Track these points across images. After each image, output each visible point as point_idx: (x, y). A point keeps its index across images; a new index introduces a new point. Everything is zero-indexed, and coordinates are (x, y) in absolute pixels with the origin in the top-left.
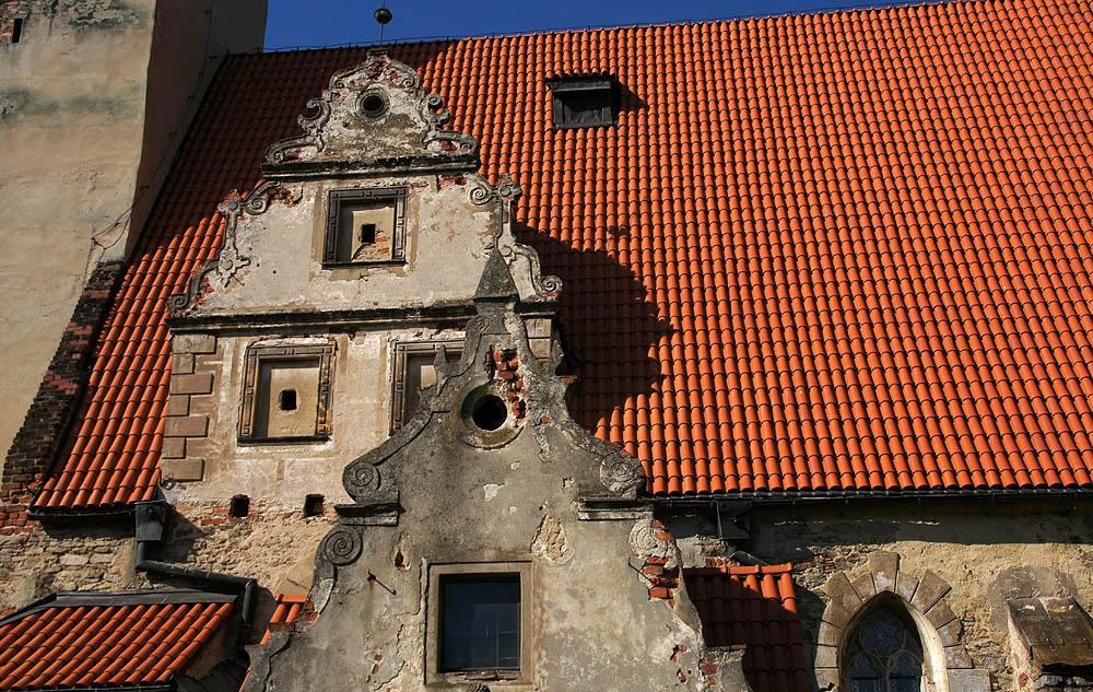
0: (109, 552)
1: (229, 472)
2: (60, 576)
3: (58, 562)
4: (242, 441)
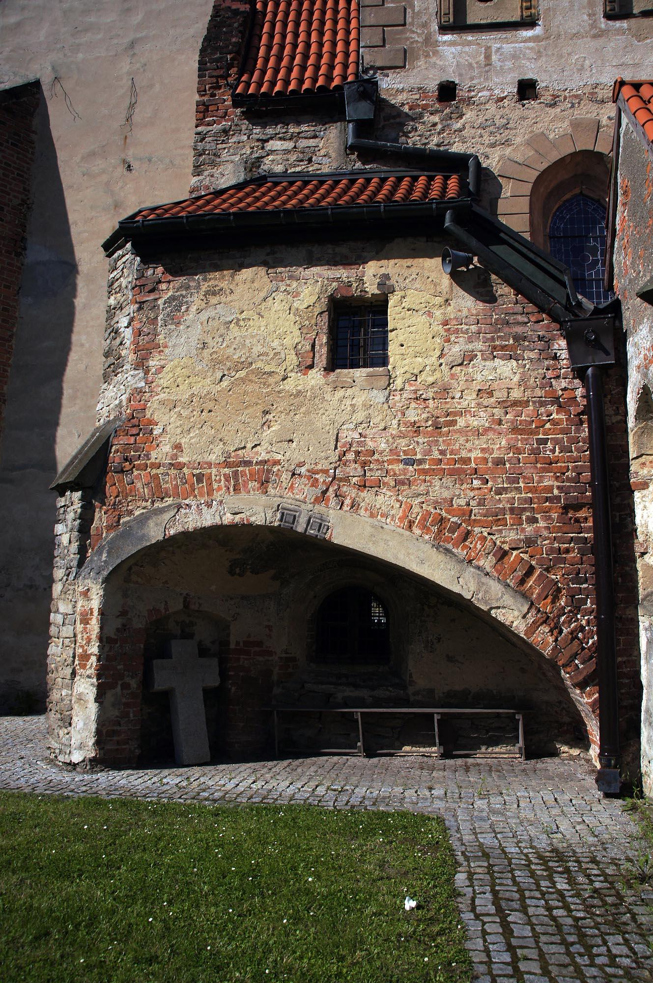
0: (315, 137)
1: (434, 59)
2: (268, 160)
3: (263, 148)
4: (444, 29)
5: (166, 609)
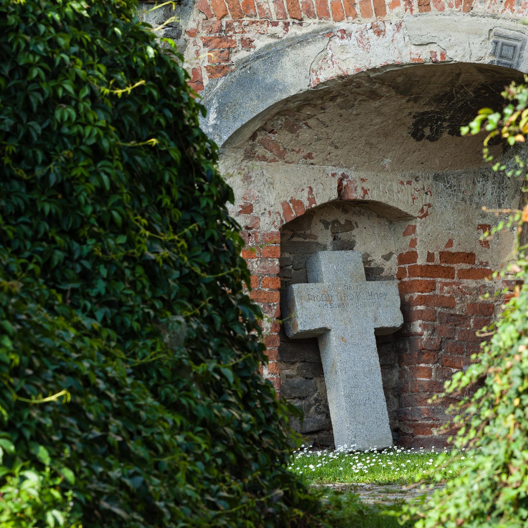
5: (312, 200)
